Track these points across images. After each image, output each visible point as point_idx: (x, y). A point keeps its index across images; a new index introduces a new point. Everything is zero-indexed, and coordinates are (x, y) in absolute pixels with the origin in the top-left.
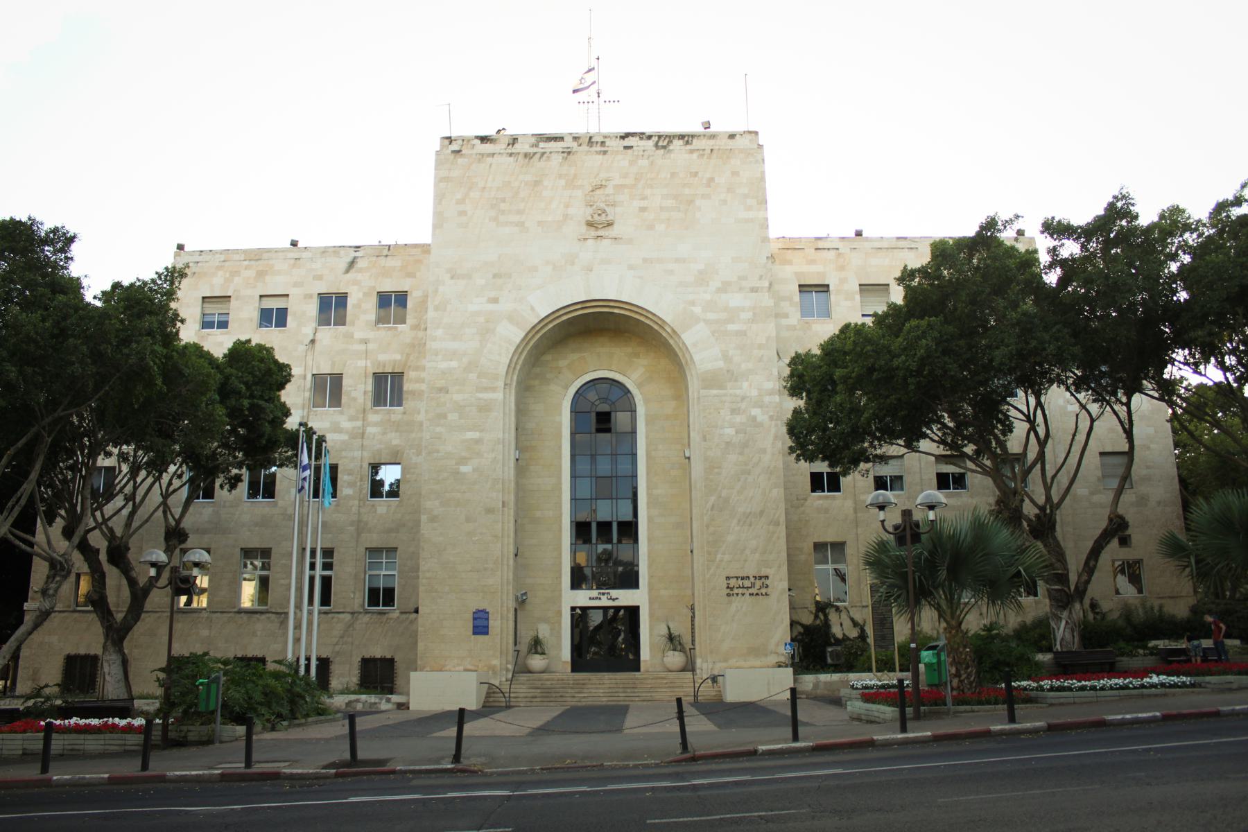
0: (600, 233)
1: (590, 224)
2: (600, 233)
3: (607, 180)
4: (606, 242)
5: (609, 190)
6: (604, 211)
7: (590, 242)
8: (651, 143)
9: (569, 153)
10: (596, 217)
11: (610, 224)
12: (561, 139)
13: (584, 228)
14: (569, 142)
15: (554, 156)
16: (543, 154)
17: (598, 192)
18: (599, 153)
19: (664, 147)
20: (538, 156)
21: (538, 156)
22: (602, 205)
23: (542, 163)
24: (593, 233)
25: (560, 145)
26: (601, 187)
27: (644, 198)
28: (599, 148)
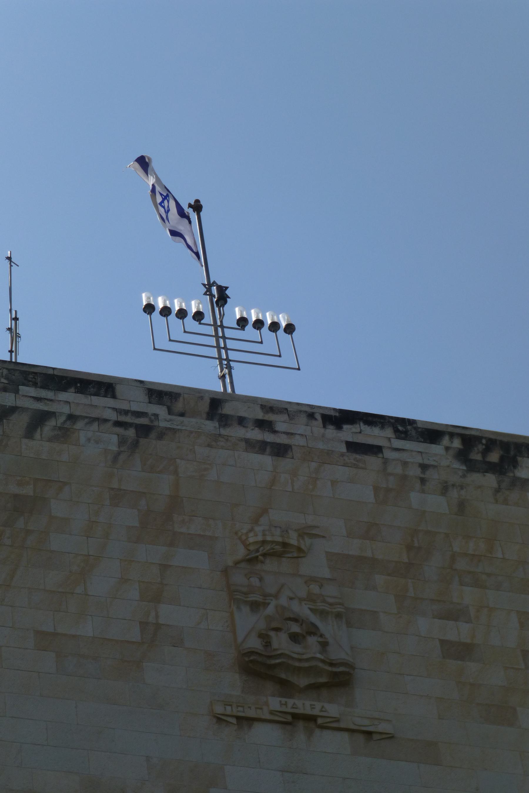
0: (304, 705)
1: (259, 668)
2: (304, 705)
3: (304, 533)
4: (330, 742)
5: (316, 565)
6: (313, 630)
7: (265, 735)
8: (437, 449)
9: (144, 431)
10: (281, 642)
11: (339, 679)
12: (105, 386)
13: (231, 684)
14: (139, 402)
15: (83, 433)
16: (40, 418)
17: (270, 565)
18: (262, 447)
19: (491, 468)
20: (20, 421)
21: (20, 421)
22: (303, 610)
23: (40, 446)
24: (275, 703)
25: (102, 406)
26: (282, 550)
27: (454, 614)
28: (256, 434)
